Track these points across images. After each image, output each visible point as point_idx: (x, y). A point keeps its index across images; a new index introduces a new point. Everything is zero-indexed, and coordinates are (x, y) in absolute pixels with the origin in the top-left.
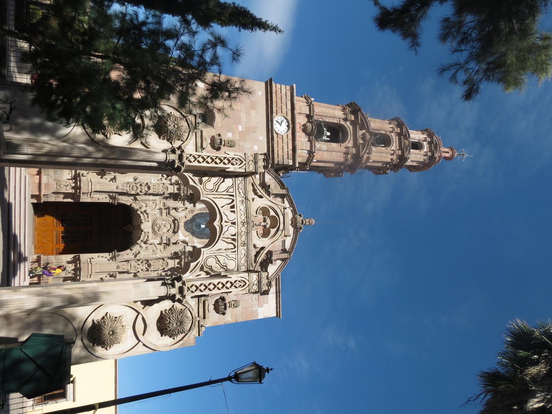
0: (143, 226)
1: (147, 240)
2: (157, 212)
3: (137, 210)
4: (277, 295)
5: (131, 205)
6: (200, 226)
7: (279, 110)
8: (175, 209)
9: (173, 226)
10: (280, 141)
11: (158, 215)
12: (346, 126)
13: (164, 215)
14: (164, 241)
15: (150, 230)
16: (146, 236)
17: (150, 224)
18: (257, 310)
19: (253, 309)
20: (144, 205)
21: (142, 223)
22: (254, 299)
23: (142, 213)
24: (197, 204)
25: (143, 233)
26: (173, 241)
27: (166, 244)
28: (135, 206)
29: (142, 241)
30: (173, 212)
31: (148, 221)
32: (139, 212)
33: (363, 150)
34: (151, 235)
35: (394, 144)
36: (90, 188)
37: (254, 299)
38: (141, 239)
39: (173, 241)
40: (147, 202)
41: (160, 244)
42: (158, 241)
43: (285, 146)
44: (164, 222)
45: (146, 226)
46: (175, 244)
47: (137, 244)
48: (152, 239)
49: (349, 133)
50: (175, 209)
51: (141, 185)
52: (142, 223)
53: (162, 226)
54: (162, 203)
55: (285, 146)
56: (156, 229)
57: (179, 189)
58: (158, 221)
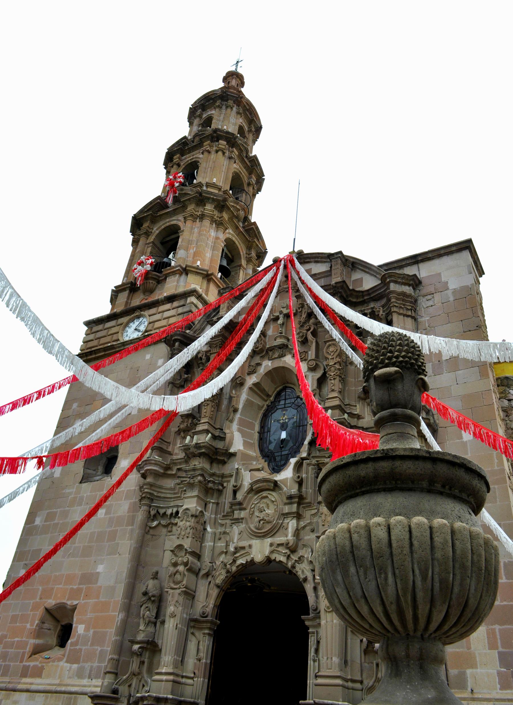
0: (259, 558)
1: (286, 545)
2: (236, 530)
3: (228, 572)
4: (423, 261)
5: (218, 586)
6: (283, 440)
7: (115, 337)
8: (235, 492)
9: (265, 494)
10: (157, 325)
11: (243, 526)
12: (158, 232)
13: (243, 514)
14: (294, 508)
15: (269, 540)
16: (280, 549)
17: (256, 543)
18: (455, 291)
19: (452, 299)
20: (222, 558)
21: (252, 560)
22: (430, 303)
23: (234, 561)
24: (232, 450)
25: (273, 557)
26: (294, 490)
27: (299, 504)
28: (221, 576)
29: (288, 557)
30: (240, 496)
31: (250, 546)
32: (234, 569)
33: (189, 194)
34: (279, 539)
35: (196, 156)
36: (164, 677)
37: (430, 303)
38: (283, 559)
39: (294, 490)
40: (217, 551)
41: (299, 516)
42: (292, 524)
43: (166, 314)
44: (257, 513)
45: (259, 550)
46: (300, 483)
47: (293, 567)
48: (287, 536)
49: (168, 224)
50: (235, 492)
51: (175, 565)
52: (252, 560)
53: (262, 515)
54: (223, 522)
55: (166, 314)
56: (268, 527)
57: (191, 486)
58: (252, 526)
